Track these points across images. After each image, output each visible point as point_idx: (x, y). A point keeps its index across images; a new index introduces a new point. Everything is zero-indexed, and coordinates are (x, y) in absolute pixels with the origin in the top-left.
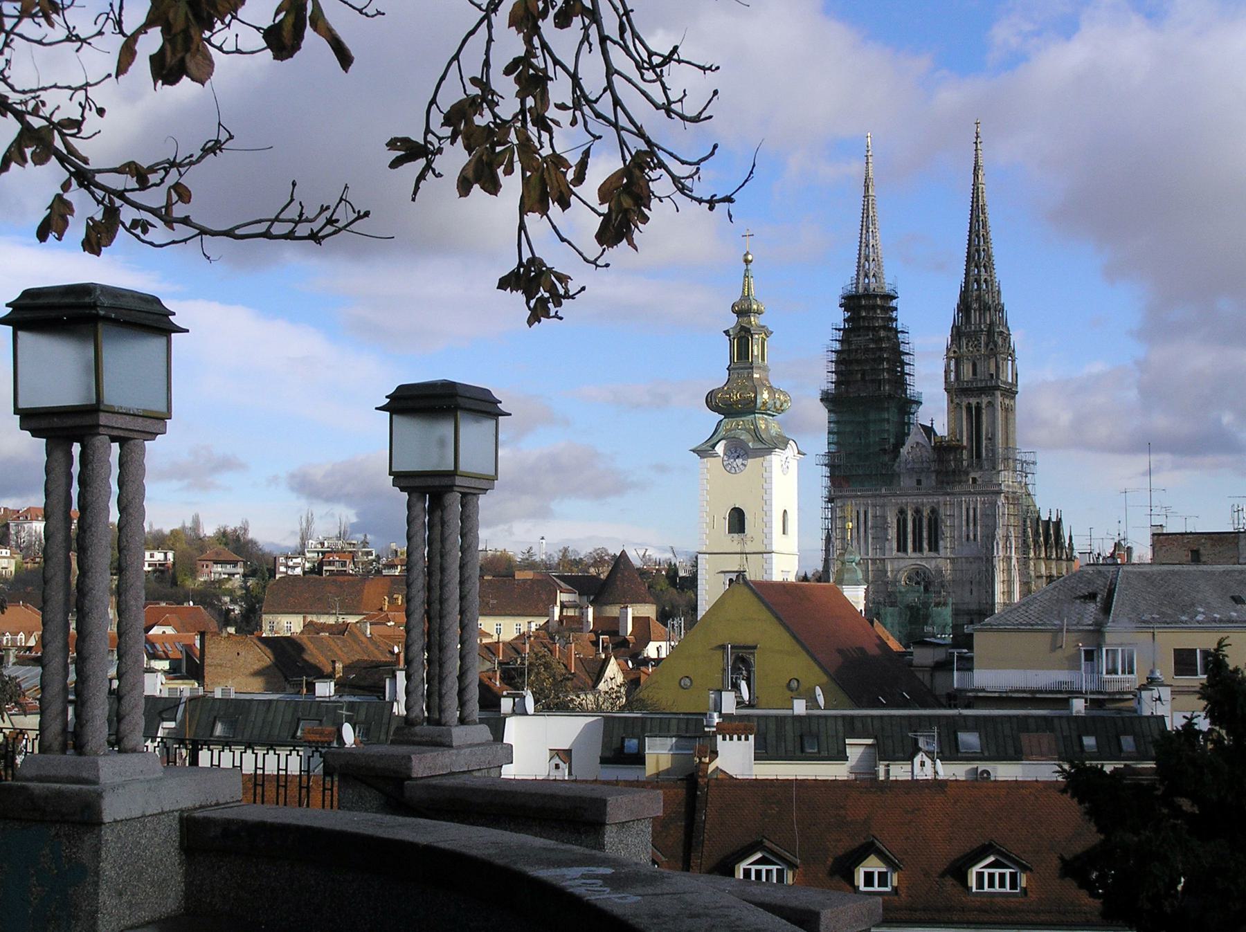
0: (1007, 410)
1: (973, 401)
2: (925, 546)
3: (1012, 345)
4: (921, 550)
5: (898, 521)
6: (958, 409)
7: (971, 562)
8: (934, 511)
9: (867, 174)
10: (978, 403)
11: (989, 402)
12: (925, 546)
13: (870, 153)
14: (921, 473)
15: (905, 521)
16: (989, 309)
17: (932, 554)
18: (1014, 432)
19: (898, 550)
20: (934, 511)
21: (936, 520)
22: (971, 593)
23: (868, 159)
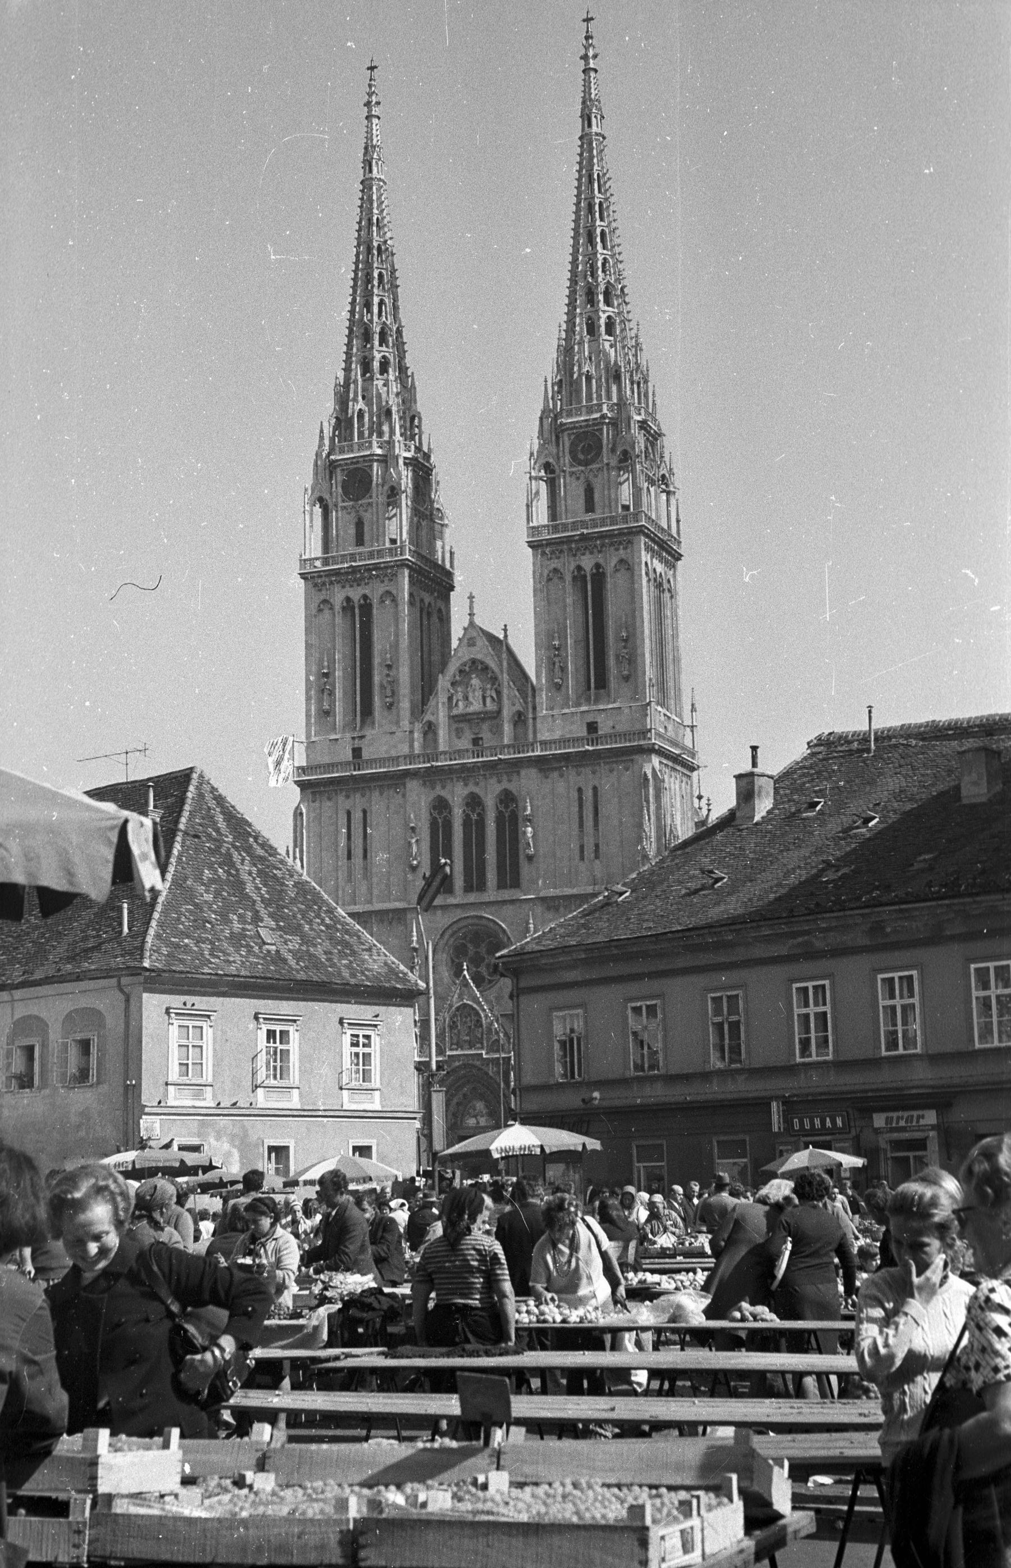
0: (659, 586)
1: (587, 563)
2: (491, 876)
3: (667, 459)
4: (481, 886)
6: (556, 580)
8: (507, 798)
9: (369, 137)
10: (598, 566)
11: (622, 561)
13: (374, 99)
15: (448, 825)
16: (617, 377)
18: (675, 636)
20: (507, 798)
23: (370, 111)
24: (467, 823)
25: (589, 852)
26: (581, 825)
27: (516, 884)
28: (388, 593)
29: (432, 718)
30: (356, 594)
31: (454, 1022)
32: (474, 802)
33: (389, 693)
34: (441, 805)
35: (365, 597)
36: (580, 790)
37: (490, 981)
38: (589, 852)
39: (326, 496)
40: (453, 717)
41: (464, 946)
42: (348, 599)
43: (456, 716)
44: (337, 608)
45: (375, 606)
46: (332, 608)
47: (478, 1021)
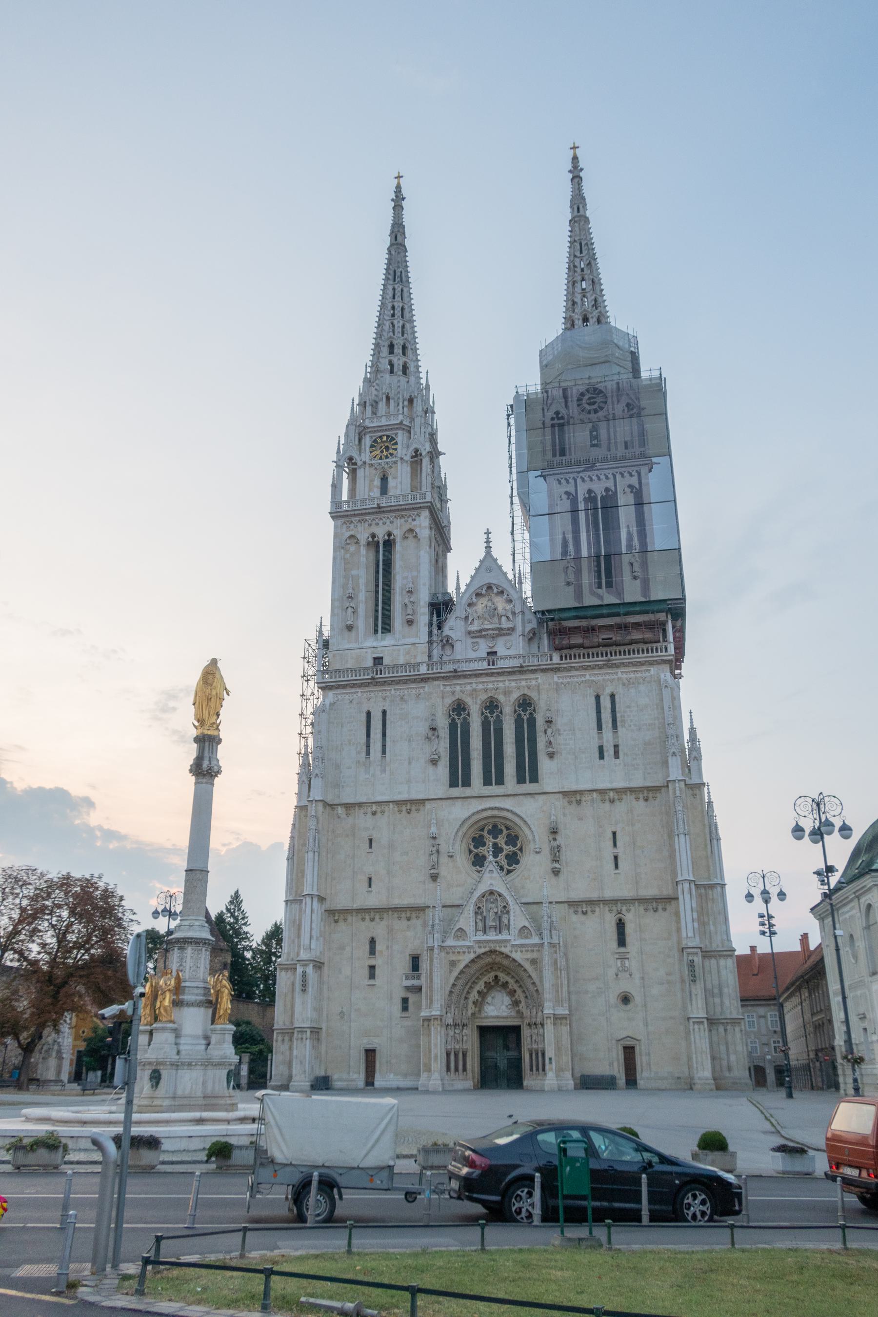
5: (453, 726)
7: (612, 801)
8: (525, 703)
12: (510, 768)
14: (493, 637)
15: (466, 726)
17: (529, 787)
19: (453, 783)
20: (525, 703)
21: (532, 722)
22: (617, 866)
24: (485, 724)
25: (609, 752)
26: (600, 727)
27: (534, 779)
28: (411, 530)
29: (451, 633)
30: (381, 533)
31: (479, 908)
32: (492, 706)
33: (410, 611)
34: (459, 708)
35: (389, 534)
36: (598, 697)
37: (509, 872)
38: (609, 752)
39: (355, 455)
40: (469, 633)
41: (482, 836)
42: (373, 536)
43: (473, 632)
44: (363, 542)
45: (398, 540)
46: (357, 543)
47: (505, 907)
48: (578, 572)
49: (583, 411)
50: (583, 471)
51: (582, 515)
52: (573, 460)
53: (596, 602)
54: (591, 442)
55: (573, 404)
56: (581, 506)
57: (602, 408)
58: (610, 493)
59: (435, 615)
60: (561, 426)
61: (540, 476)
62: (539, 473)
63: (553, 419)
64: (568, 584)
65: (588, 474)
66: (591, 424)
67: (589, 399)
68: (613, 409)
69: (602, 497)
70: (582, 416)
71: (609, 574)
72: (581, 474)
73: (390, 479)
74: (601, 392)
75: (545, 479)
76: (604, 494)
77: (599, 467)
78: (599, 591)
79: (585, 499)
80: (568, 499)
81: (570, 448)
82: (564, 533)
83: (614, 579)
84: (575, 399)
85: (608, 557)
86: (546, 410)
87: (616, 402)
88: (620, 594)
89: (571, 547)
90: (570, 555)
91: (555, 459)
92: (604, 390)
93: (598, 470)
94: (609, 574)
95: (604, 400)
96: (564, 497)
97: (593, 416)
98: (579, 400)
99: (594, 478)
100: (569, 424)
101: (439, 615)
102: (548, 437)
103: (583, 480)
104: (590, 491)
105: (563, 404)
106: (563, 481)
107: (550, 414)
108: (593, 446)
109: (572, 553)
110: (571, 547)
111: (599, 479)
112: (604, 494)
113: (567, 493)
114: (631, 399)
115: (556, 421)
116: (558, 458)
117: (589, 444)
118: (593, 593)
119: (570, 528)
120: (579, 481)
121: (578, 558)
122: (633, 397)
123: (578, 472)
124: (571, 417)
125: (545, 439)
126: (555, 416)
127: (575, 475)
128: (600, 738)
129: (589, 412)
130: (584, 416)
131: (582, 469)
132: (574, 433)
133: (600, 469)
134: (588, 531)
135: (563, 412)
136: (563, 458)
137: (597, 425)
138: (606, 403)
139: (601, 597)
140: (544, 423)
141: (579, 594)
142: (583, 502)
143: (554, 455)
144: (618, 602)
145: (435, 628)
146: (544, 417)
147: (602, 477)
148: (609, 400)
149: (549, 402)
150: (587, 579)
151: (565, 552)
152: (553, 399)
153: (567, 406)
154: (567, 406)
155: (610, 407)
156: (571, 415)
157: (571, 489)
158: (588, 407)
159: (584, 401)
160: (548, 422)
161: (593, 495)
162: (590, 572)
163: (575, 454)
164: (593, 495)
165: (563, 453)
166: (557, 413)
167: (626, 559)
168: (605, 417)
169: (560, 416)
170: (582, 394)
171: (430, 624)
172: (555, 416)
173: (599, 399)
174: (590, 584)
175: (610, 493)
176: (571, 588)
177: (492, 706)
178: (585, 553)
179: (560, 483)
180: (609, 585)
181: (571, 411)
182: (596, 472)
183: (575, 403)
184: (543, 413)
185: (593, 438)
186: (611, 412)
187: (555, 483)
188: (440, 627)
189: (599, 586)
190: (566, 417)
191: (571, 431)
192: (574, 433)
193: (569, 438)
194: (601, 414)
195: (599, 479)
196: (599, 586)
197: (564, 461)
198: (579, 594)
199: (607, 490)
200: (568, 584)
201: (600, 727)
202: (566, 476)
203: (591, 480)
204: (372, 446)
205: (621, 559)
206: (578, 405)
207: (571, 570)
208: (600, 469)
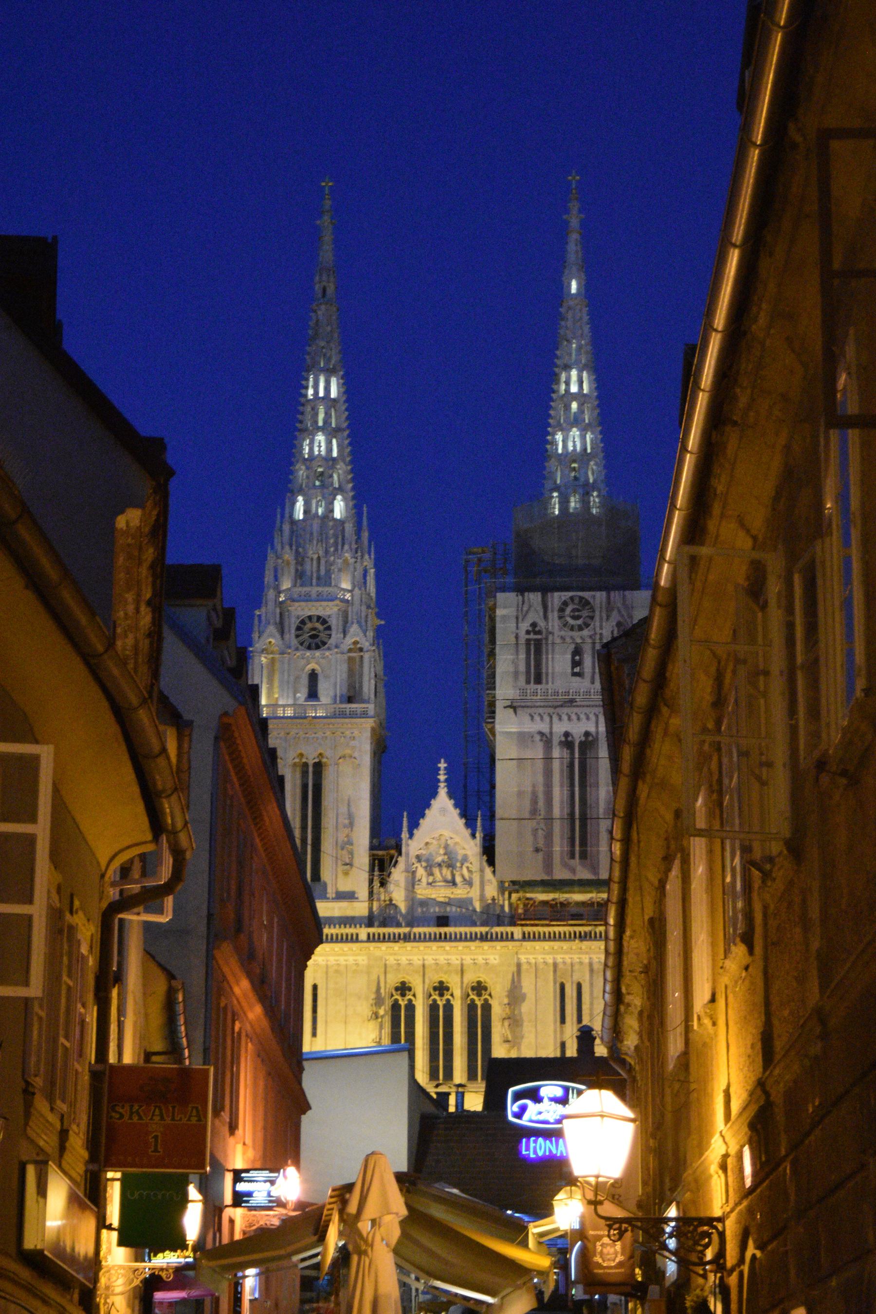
5: (395, 1007)
21: (487, 1007)
26: (563, 1020)
48: (549, 837)
49: (565, 625)
50: (562, 706)
51: (556, 765)
52: (550, 691)
53: (565, 875)
54: (573, 668)
55: (554, 616)
56: (556, 752)
57: (587, 625)
58: (590, 738)
59: (376, 868)
60: (538, 644)
61: (510, 707)
62: (508, 703)
63: (528, 632)
64: (537, 850)
65: (565, 710)
66: (573, 646)
67: (573, 610)
68: (601, 628)
69: (581, 743)
70: (563, 633)
71: (584, 842)
72: (559, 710)
73: (321, 680)
74: (587, 603)
75: (515, 712)
76: (583, 739)
77: (578, 703)
78: (572, 862)
79: (561, 743)
80: (541, 740)
81: (547, 674)
82: (534, 786)
83: (589, 849)
84: (556, 607)
85: (584, 819)
86: (520, 619)
87: (605, 617)
88: (595, 869)
89: (541, 804)
90: (540, 815)
91: (528, 687)
92: (591, 601)
93: (577, 706)
94: (584, 842)
95: (591, 614)
96: (538, 738)
97: (575, 634)
98: (561, 610)
99: (574, 717)
100: (547, 639)
101: (382, 869)
102: (522, 656)
103: (560, 719)
104: (567, 734)
105: (541, 614)
106: (537, 718)
107: (525, 626)
108: (574, 674)
109: (543, 813)
110: (541, 804)
111: (579, 719)
112: (583, 739)
113: (541, 734)
114: (622, 616)
115: (532, 636)
116: (533, 686)
117: (569, 670)
118: (565, 865)
119: (540, 779)
120: (555, 718)
121: (549, 819)
122: (625, 614)
123: (556, 707)
124: (551, 633)
125: (517, 658)
126: (530, 629)
127: (551, 710)
128: (562, 1032)
129: (572, 628)
130: (567, 634)
131: (559, 703)
132: (553, 654)
133: (580, 706)
134: (562, 786)
135: (542, 624)
136: (539, 687)
137: (582, 649)
138: (592, 618)
139: (573, 871)
140: (517, 637)
141: (548, 865)
142: (558, 748)
143: (528, 682)
144: (593, 877)
145: (376, 884)
146: (517, 628)
147: (582, 716)
148: (597, 613)
149: (525, 609)
150: (559, 847)
151: (534, 811)
152: (530, 606)
153: (546, 617)
154: (546, 617)
155: (598, 624)
156: (550, 628)
157: (544, 727)
158: (569, 619)
159: (568, 610)
160: (523, 637)
161: (570, 739)
162: (562, 838)
163: (553, 683)
164: (570, 739)
165: (538, 681)
166: (534, 625)
167: (604, 825)
168: (591, 637)
169: (537, 629)
170: (565, 604)
171: (371, 881)
172: (530, 629)
173: (585, 613)
174: (562, 852)
175: (590, 738)
176: (540, 856)
177: (441, 988)
178: (556, 812)
179: (532, 717)
180: (584, 856)
181: (550, 624)
182: (575, 710)
183: (556, 614)
184: (517, 623)
185: (575, 664)
186: (598, 630)
187: (528, 718)
188: (383, 884)
189: (572, 856)
190: (544, 631)
191: (550, 651)
192: (553, 654)
193: (547, 658)
194: (586, 632)
195: (579, 719)
196: (572, 856)
197: (539, 691)
198: (548, 865)
199: (587, 734)
200: (537, 850)
201: (563, 1020)
202: (541, 710)
203: (569, 719)
204: (298, 628)
205: (598, 824)
206: (560, 618)
207: (540, 832)
208: (580, 706)
